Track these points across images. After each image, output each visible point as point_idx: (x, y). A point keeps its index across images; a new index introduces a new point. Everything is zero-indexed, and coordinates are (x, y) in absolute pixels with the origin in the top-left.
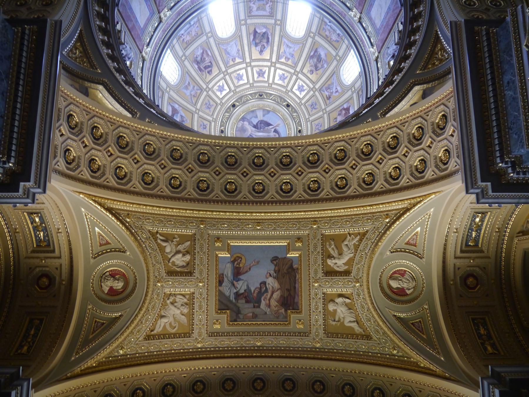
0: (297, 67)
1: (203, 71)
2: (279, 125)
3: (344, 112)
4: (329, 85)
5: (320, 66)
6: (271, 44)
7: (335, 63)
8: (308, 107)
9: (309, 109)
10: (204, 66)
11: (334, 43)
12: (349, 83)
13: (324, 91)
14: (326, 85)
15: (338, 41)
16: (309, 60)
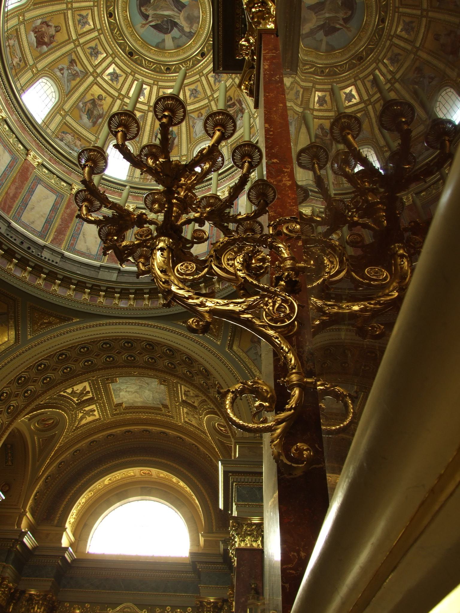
0: (121, 104)
1: (237, 100)
2: (142, 27)
3: (46, 40)
4: (74, 80)
5: (88, 104)
6: (153, 134)
7: (67, 107)
8: (103, 51)
9: (100, 49)
10: (235, 107)
11: (70, 131)
12: (43, 80)
13: (81, 71)
14: (78, 79)
15: (63, 132)
16: (104, 113)
